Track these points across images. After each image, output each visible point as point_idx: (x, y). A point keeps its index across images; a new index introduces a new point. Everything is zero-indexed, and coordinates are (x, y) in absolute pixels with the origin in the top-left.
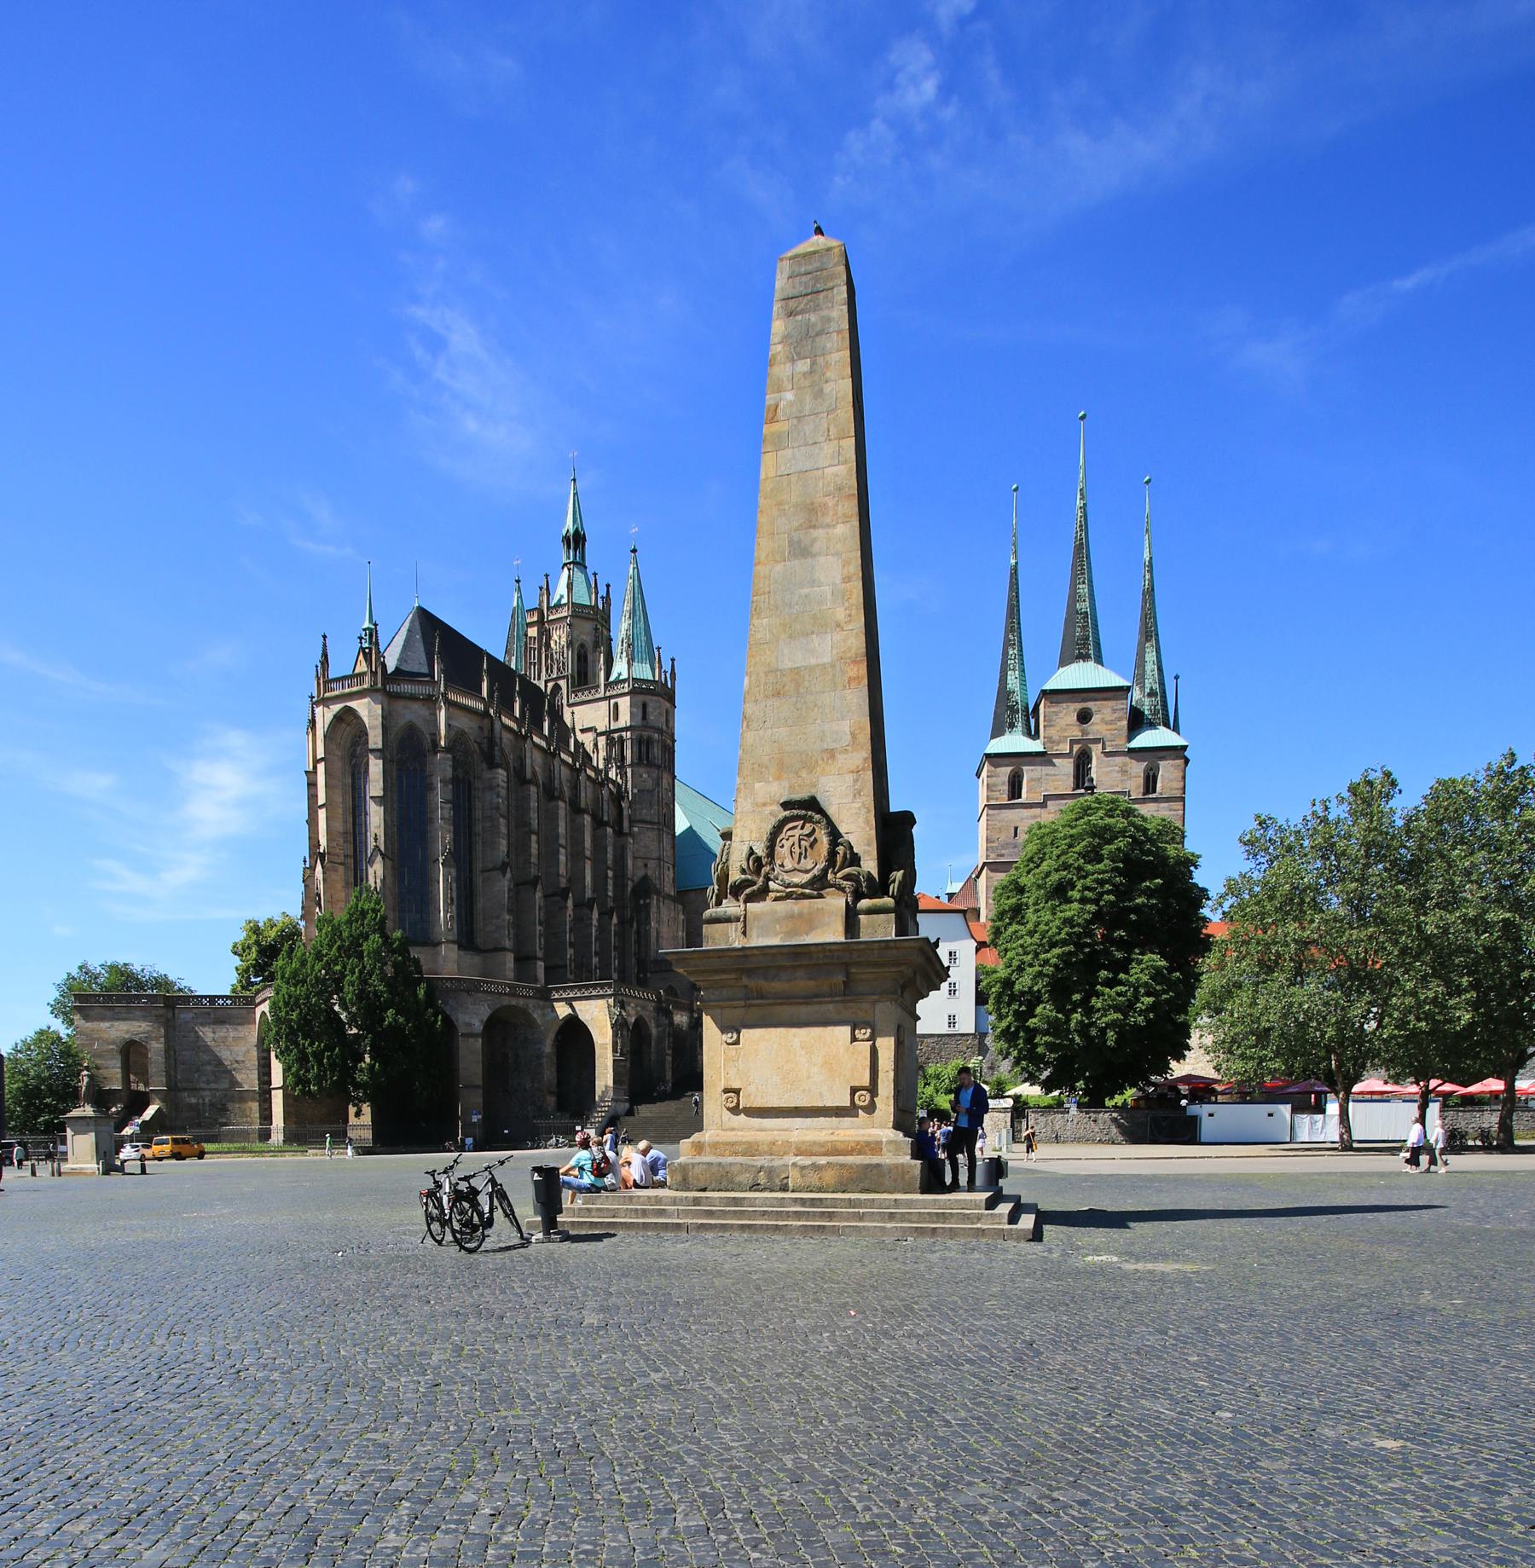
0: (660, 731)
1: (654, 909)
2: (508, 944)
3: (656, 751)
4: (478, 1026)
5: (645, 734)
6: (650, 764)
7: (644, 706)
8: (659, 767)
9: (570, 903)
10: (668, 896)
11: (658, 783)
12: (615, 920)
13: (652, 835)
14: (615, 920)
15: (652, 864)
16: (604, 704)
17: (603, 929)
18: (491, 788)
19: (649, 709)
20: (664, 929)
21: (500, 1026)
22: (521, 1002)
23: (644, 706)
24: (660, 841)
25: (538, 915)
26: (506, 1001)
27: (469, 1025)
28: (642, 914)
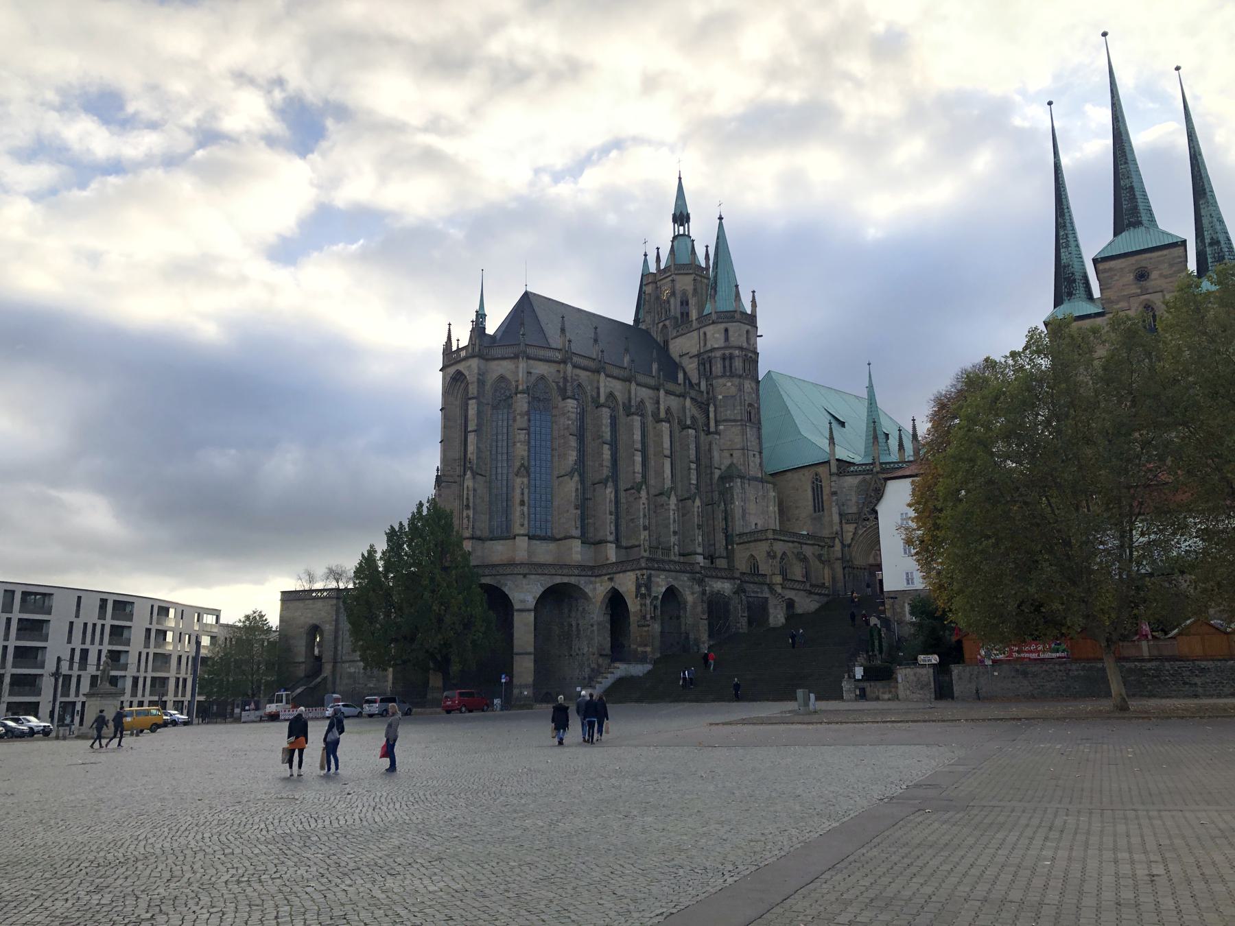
0: (741, 348)
1: (737, 491)
2: (577, 533)
3: (738, 364)
4: (531, 603)
5: (727, 352)
6: (732, 375)
7: (726, 330)
8: (740, 376)
9: (643, 493)
10: (756, 479)
11: (740, 389)
12: (698, 502)
13: (736, 430)
14: (698, 502)
15: (737, 454)
16: (695, 334)
17: (683, 512)
18: (564, 414)
19: (730, 333)
20: (752, 507)
21: (558, 597)
22: (573, 580)
23: (726, 330)
24: (744, 433)
25: (609, 506)
26: (558, 580)
27: (523, 601)
28: (726, 496)
